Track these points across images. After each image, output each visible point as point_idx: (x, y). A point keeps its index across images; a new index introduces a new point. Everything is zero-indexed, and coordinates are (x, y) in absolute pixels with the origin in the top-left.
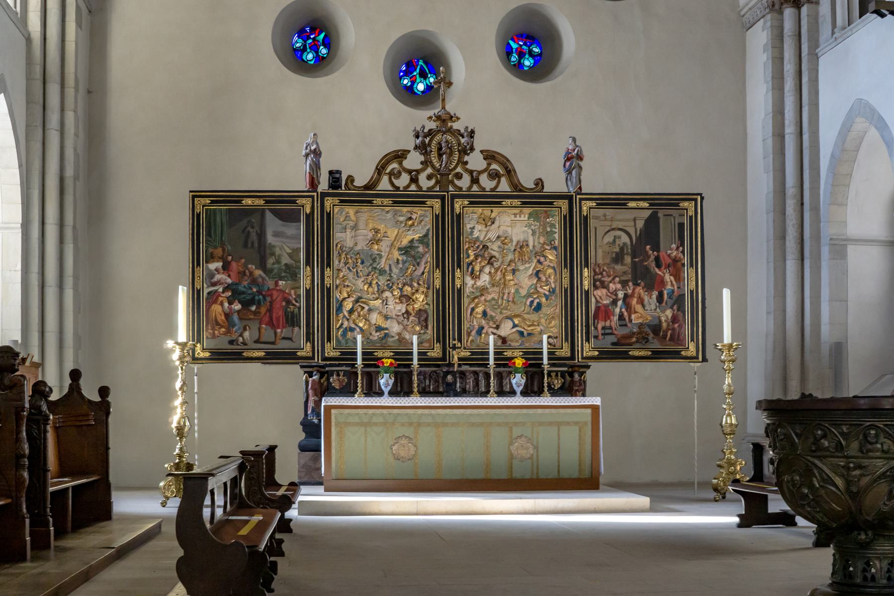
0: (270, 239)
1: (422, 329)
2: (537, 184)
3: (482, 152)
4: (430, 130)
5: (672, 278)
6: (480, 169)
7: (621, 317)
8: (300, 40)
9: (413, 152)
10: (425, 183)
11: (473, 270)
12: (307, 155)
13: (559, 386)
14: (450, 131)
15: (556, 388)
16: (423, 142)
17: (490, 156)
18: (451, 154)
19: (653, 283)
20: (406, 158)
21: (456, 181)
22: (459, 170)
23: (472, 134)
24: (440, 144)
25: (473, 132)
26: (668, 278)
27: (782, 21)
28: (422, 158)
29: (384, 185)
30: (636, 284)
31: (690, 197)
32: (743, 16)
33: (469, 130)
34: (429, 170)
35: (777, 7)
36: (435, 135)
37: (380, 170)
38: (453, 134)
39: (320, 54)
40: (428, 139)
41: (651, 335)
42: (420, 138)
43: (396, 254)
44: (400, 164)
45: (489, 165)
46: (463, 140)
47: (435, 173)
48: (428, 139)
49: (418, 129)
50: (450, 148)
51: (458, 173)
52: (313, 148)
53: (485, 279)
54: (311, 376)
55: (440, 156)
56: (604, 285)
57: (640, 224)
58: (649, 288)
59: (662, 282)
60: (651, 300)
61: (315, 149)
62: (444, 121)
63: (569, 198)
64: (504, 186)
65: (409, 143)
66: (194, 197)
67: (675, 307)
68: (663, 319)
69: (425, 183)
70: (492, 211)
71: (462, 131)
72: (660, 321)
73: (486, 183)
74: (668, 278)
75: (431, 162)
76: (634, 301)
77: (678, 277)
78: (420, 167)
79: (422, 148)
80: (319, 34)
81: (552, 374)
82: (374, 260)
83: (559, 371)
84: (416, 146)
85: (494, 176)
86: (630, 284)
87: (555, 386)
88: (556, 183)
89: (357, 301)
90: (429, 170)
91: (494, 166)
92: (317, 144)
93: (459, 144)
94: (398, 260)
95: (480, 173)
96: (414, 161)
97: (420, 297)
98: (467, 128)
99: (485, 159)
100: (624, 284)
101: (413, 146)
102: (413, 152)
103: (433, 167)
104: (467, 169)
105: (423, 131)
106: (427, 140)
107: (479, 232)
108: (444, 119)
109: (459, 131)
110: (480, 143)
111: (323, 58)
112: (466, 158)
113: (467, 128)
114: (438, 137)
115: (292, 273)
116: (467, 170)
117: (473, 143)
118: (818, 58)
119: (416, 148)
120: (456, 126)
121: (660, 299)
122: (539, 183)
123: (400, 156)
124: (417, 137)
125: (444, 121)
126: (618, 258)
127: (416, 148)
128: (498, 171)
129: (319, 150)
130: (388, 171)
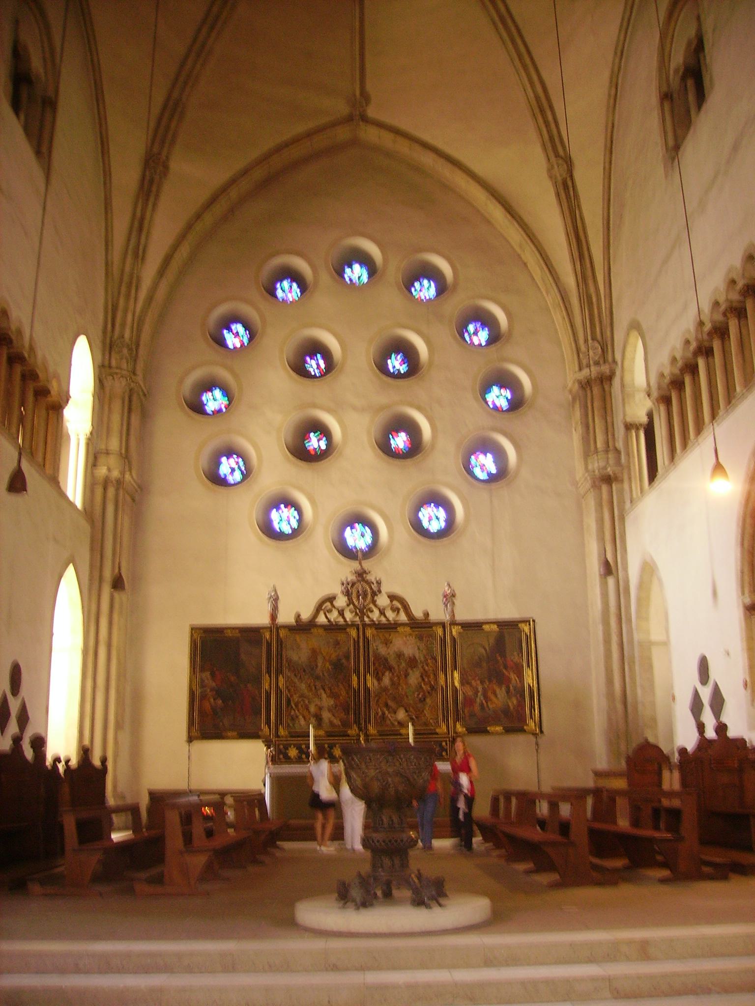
0: (243, 657)
1: (345, 715)
2: (424, 614)
5: (515, 676)
7: (482, 705)
10: (349, 616)
11: (378, 673)
17: (392, 597)
19: (502, 680)
21: (369, 613)
23: (379, 583)
26: (513, 676)
27: (601, 493)
29: (322, 619)
30: (490, 681)
31: (526, 621)
32: (580, 487)
37: (319, 608)
41: (503, 716)
43: (328, 665)
53: (386, 680)
54: (270, 748)
56: (469, 683)
57: (492, 640)
58: (500, 684)
59: (509, 680)
60: (501, 693)
63: (443, 625)
64: (403, 617)
65: (337, 590)
66: (192, 629)
67: (518, 696)
68: (510, 704)
69: (349, 616)
70: (390, 635)
72: (508, 706)
73: (391, 615)
74: (513, 676)
76: (490, 694)
77: (520, 675)
79: (348, 594)
82: (312, 669)
85: (397, 610)
86: (487, 682)
88: (438, 614)
89: (300, 697)
94: (328, 668)
96: (341, 601)
97: (344, 693)
98: (376, 579)
100: (482, 682)
103: (354, 605)
107: (382, 650)
108: (361, 575)
110: (385, 589)
113: (376, 579)
115: (258, 681)
116: (376, 606)
121: (508, 692)
122: (427, 615)
123: (331, 599)
124: (343, 584)
126: (478, 664)
130: (323, 608)
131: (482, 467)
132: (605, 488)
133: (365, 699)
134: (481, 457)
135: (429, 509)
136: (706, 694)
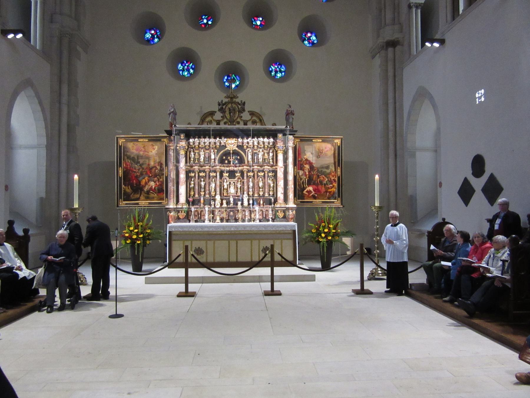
3: (249, 112)
4: (225, 102)
6: (248, 119)
8: (182, 67)
9: (217, 112)
12: (170, 114)
13: (282, 216)
14: (235, 103)
15: (281, 218)
16: (222, 108)
17: (252, 113)
18: (235, 113)
20: (214, 115)
22: (239, 120)
23: (244, 104)
24: (229, 108)
25: (244, 103)
28: (222, 115)
33: (243, 102)
34: (225, 120)
35: (385, 47)
36: (228, 104)
38: (236, 104)
39: (190, 72)
40: (225, 106)
42: (221, 106)
44: (212, 118)
45: (252, 117)
46: (240, 107)
47: (228, 121)
48: (225, 106)
49: (220, 102)
50: (234, 110)
51: (237, 121)
52: (172, 111)
55: (230, 113)
61: (173, 111)
62: (232, 98)
65: (216, 108)
71: (240, 102)
75: (226, 117)
78: (221, 119)
79: (222, 110)
80: (190, 64)
81: (279, 211)
83: (282, 210)
84: (219, 109)
87: (280, 216)
90: (225, 120)
91: (254, 118)
92: (175, 109)
93: (238, 108)
95: (247, 121)
98: (242, 101)
99: (250, 115)
101: (218, 109)
102: (217, 112)
104: (242, 119)
105: (222, 103)
106: (224, 107)
109: (238, 102)
110: (247, 108)
111: (191, 74)
112: (242, 115)
113: (242, 101)
114: (230, 106)
116: (242, 120)
117: (244, 108)
118: (403, 69)
119: (219, 110)
120: (237, 100)
123: (212, 113)
124: (219, 105)
125: (232, 98)
127: (219, 110)
128: (256, 120)
129: (175, 112)
131: (309, 39)
132: (390, 49)
133: (117, 160)
134: (309, 35)
135: (276, 67)
136: (478, 184)
